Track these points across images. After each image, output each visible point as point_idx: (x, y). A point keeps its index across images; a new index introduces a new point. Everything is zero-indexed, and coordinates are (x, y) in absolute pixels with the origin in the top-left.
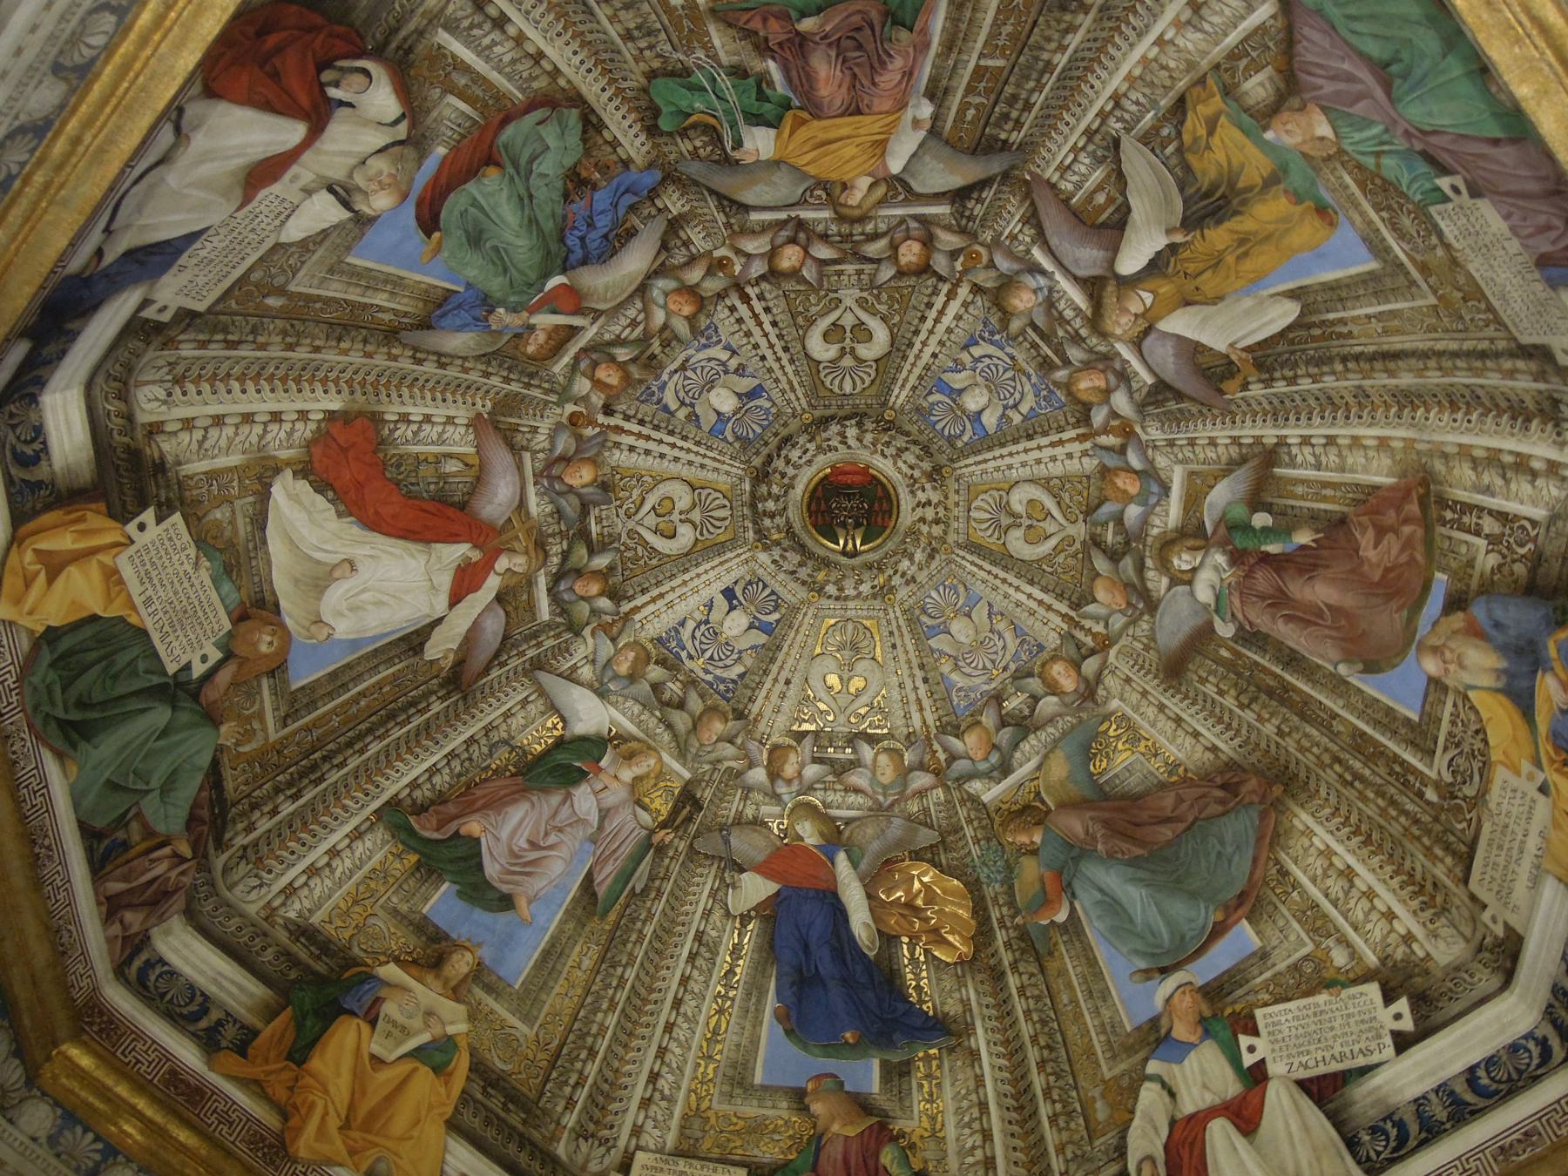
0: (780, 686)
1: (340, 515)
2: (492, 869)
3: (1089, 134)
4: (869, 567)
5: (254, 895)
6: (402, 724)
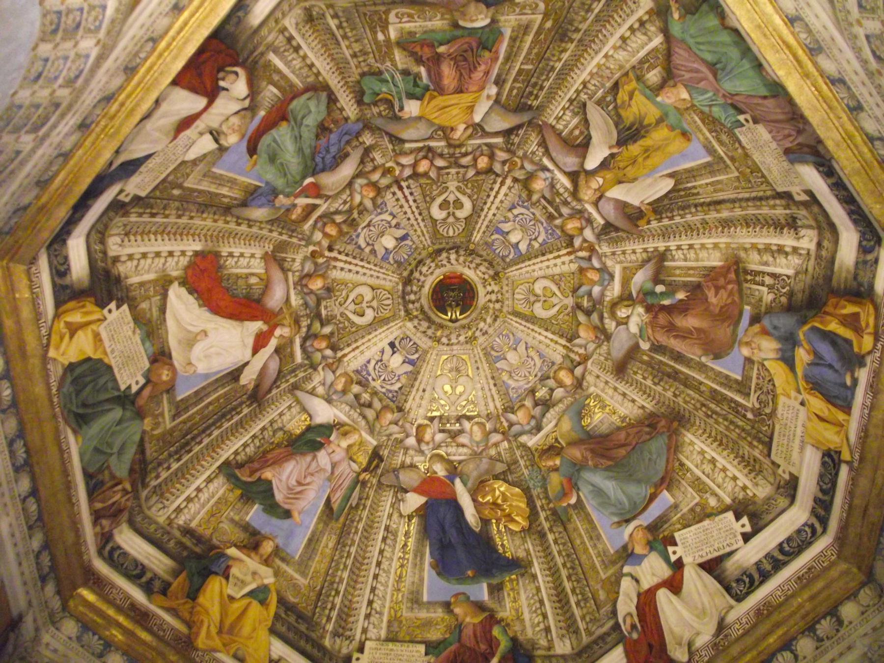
0: (420, 393)
1: (200, 306)
2: (279, 497)
3: (571, 101)
4: (464, 327)
5: (161, 513)
6: (229, 420)
